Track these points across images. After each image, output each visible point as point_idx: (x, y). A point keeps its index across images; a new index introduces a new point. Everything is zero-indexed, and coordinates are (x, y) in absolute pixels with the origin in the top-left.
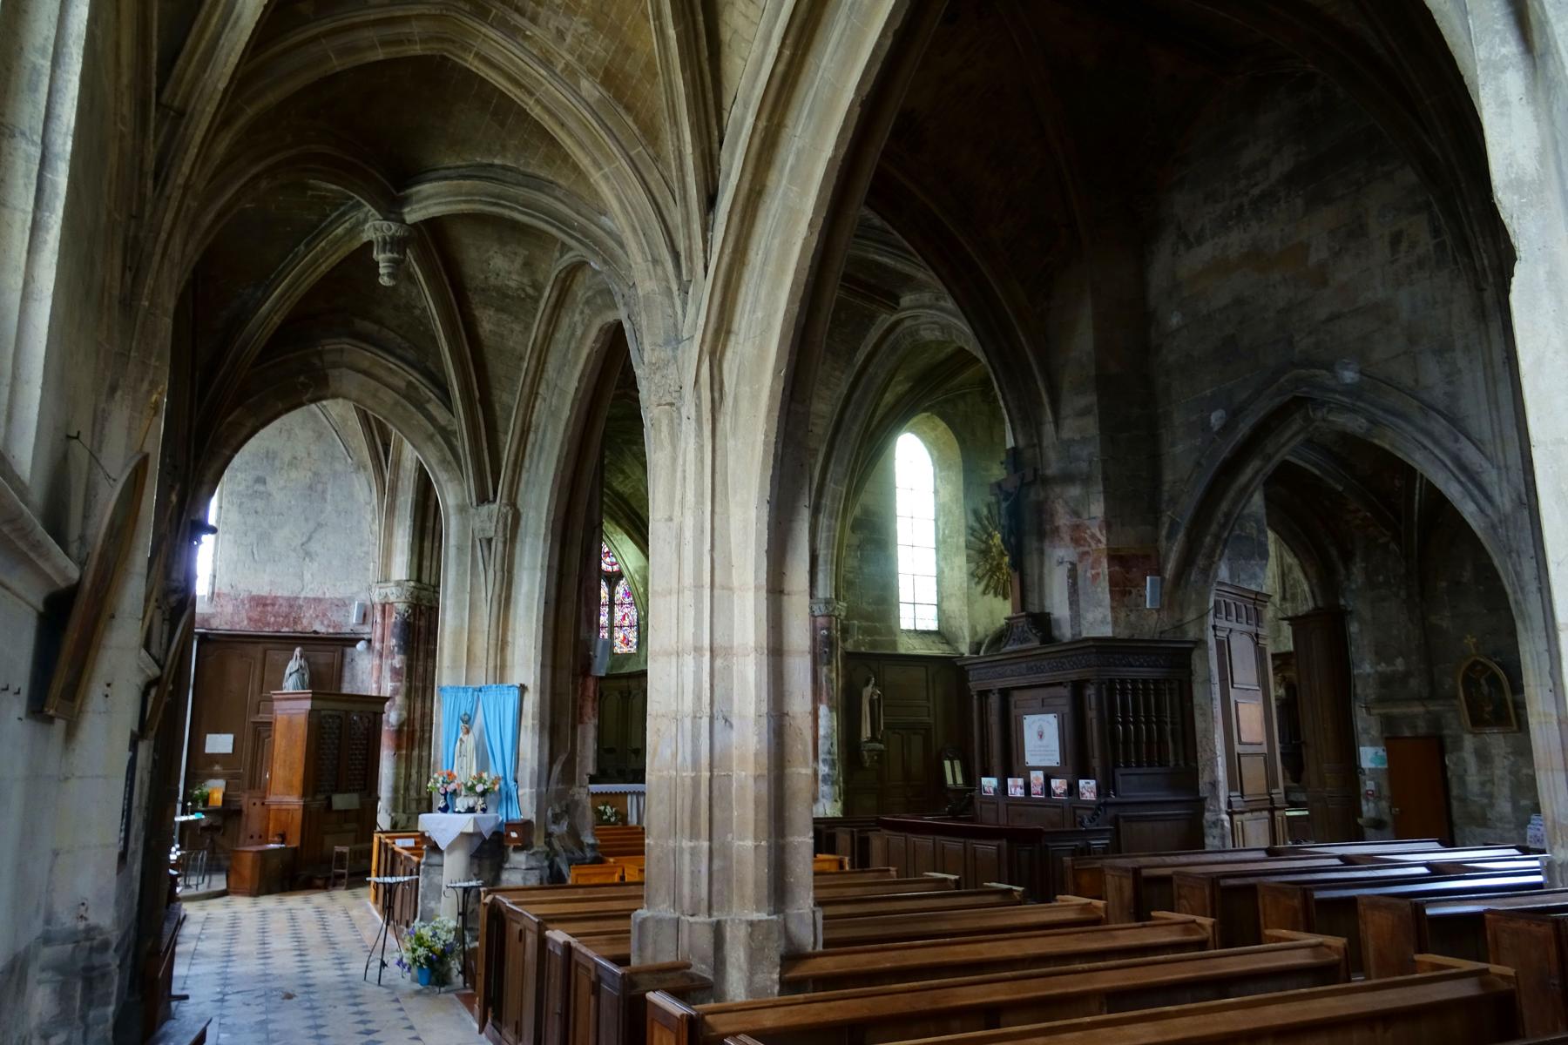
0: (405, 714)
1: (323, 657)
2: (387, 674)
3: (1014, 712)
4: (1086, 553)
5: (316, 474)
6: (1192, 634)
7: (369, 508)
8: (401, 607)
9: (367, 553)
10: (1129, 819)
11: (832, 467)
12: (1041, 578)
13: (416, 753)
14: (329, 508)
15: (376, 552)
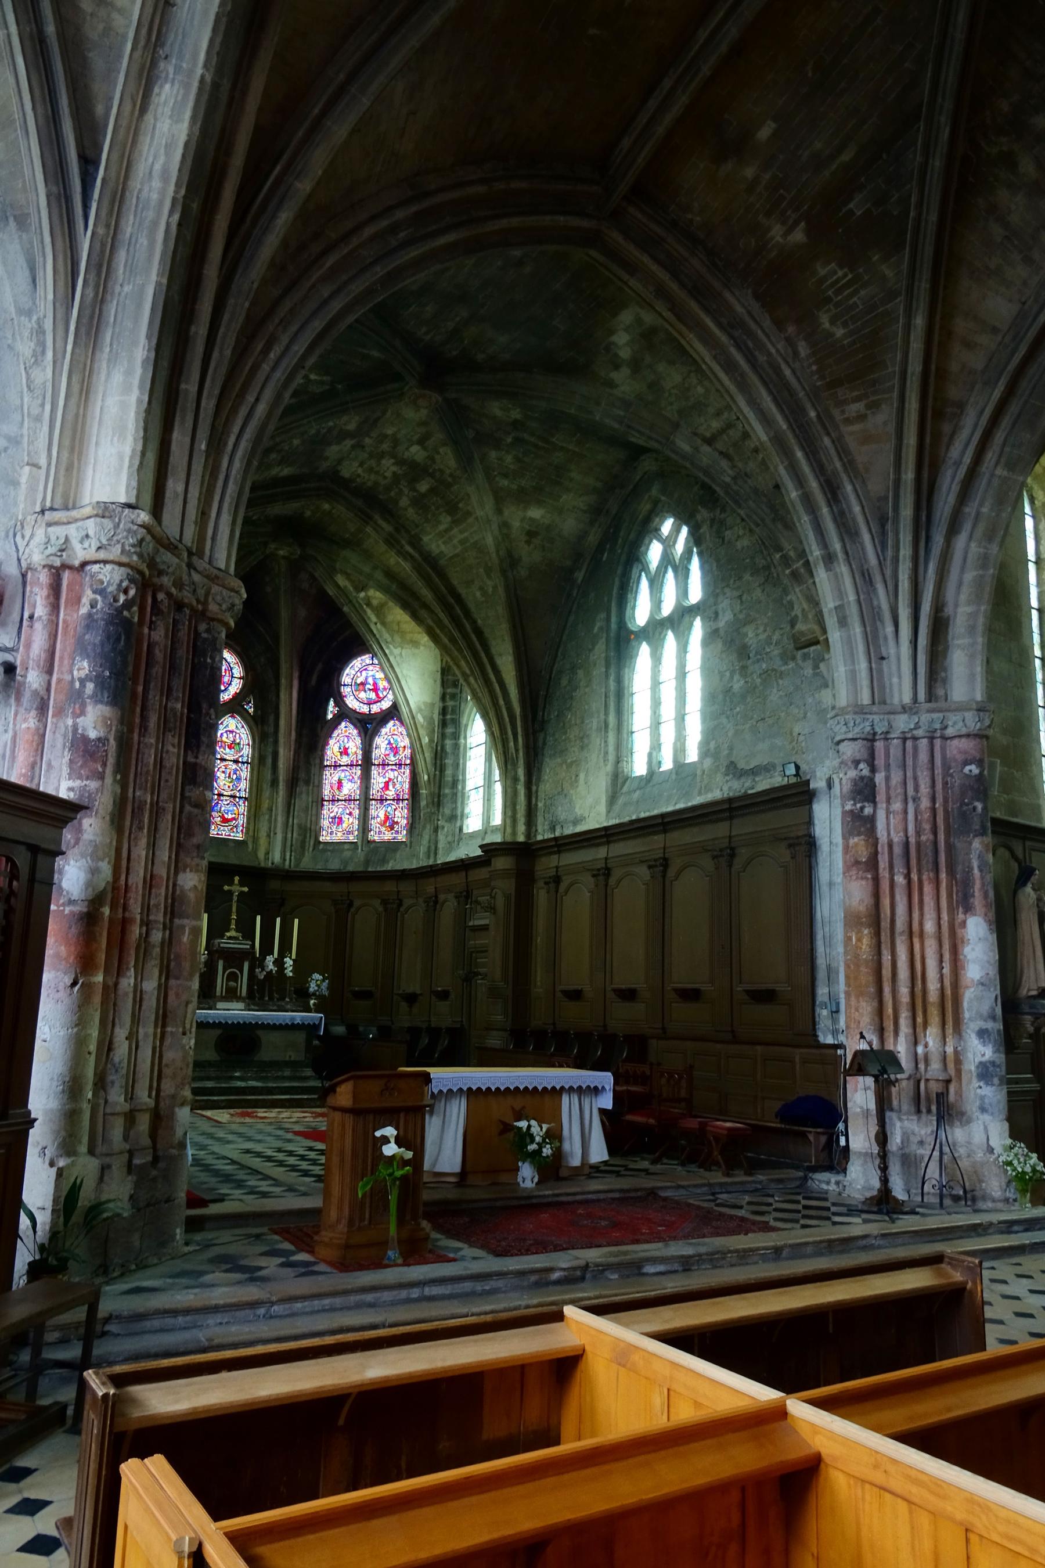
0: (106, 868)
7: (28, 324)
8: (110, 576)
9: (15, 441)
11: (999, 437)
13: (128, 982)
15: (41, 441)
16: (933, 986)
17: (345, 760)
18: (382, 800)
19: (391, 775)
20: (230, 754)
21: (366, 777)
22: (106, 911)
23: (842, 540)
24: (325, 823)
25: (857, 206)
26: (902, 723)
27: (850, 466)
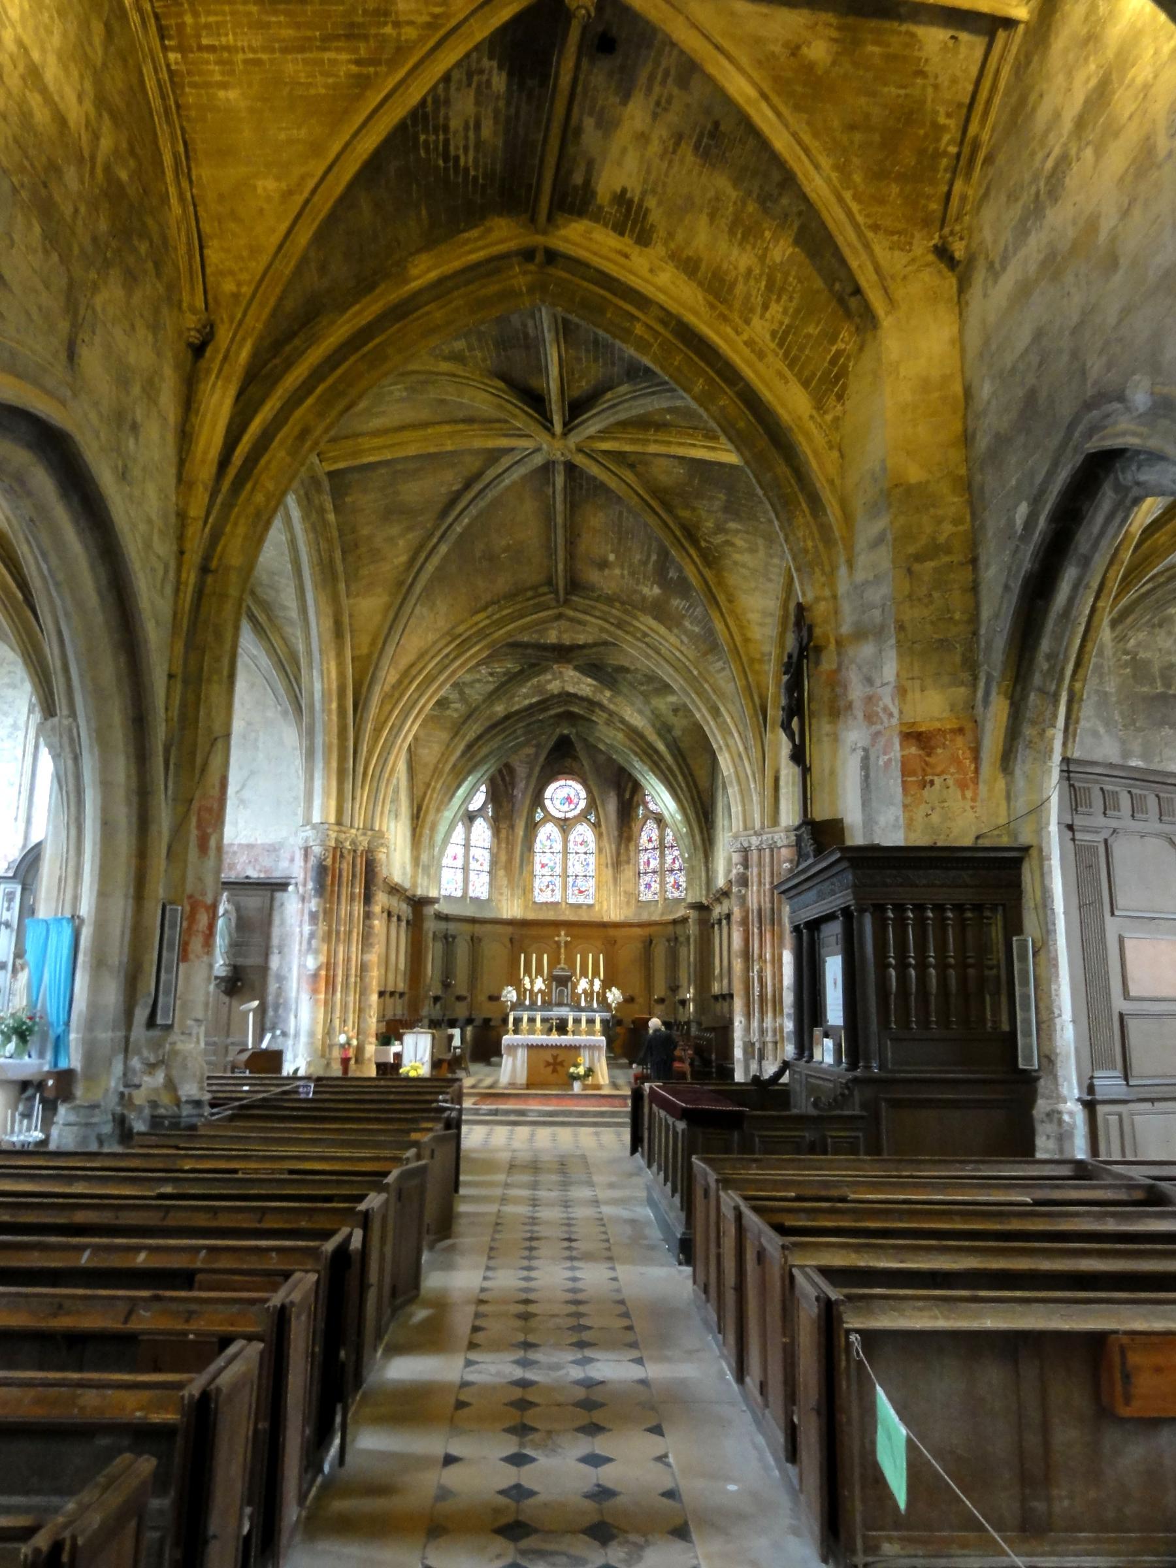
1: (253, 902)
2: (306, 917)
3: (823, 951)
4: (878, 734)
5: (249, 724)
6: (1025, 838)
8: (317, 850)
10: (896, 1104)
12: (833, 773)
14: (261, 756)
16: (769, 989)
17: (650, 846)
18: (672, 871)
19: (677, 853)
20: (582, 849)
21: (662, 856)
22: (323, 973)
23: (724, 739)
24: (642, 888)
25: (673, 574)
26: (755, 841)
27: (721, 695)
